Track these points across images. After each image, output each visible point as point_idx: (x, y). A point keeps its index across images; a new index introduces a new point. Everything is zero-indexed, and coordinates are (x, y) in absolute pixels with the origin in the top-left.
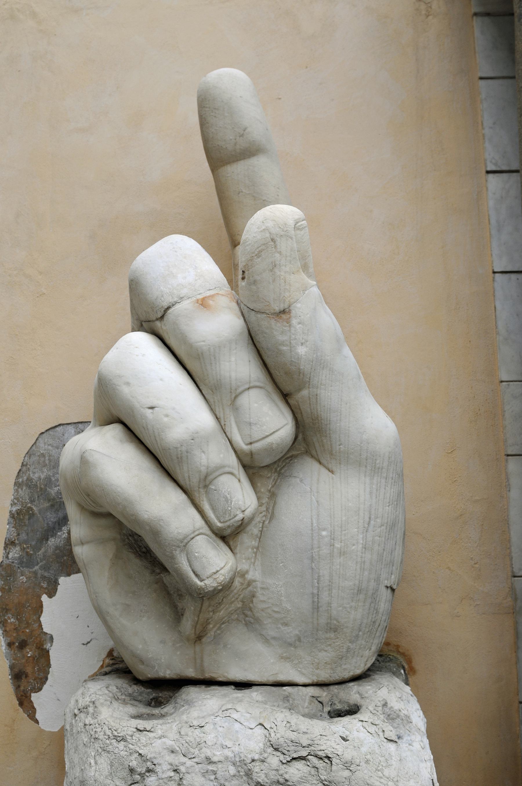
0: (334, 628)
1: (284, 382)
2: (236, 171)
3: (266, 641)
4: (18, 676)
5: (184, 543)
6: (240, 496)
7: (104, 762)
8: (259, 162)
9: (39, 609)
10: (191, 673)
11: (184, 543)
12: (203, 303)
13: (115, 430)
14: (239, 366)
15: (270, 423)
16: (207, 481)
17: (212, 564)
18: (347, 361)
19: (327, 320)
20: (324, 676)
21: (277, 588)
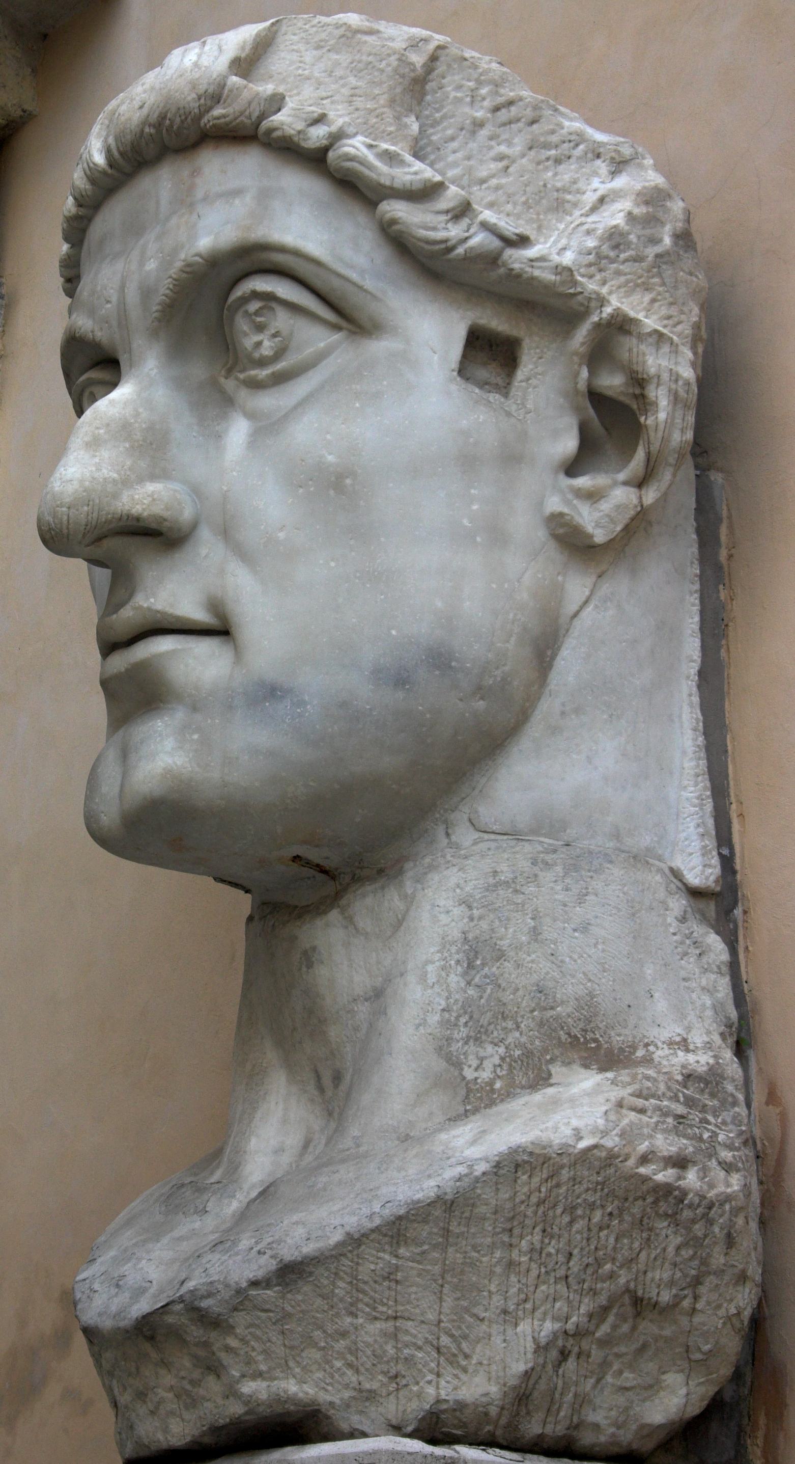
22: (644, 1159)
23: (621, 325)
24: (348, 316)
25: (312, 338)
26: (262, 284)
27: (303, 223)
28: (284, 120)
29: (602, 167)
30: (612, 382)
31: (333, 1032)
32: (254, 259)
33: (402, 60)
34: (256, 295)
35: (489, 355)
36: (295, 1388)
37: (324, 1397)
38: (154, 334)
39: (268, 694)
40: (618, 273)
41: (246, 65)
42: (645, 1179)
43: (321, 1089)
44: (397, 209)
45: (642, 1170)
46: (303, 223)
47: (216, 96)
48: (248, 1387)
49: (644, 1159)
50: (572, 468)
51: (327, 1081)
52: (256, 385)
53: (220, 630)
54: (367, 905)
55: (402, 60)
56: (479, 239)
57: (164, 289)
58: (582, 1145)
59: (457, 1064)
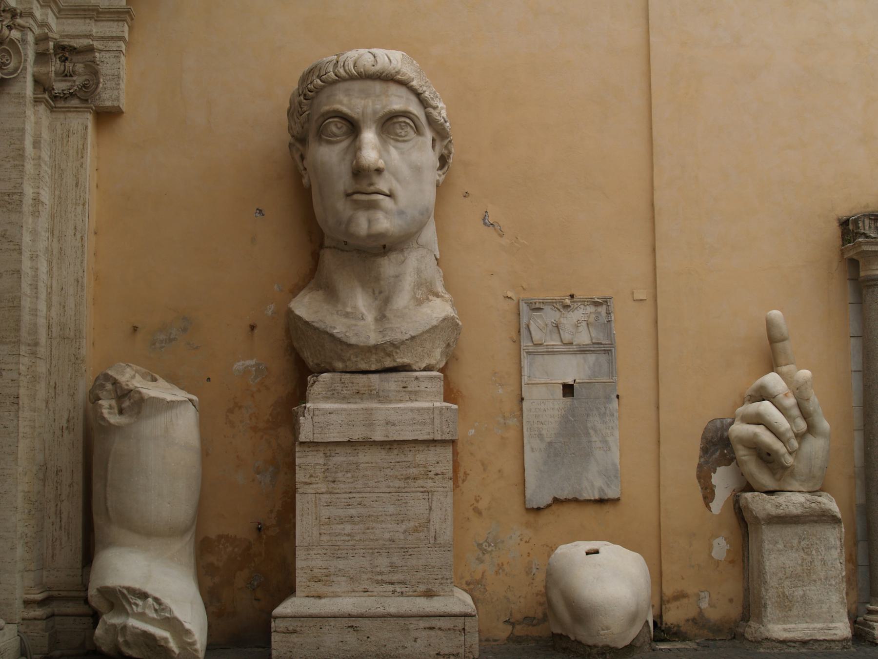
0: (814, 477)
1: (806, 415)
2: (779, 345)
3: (797, 480)
4: (705, 498)
5: (783, 455)
6: (795, 443)
7: (769, 505)
8: (786, 342)
9: (711, 477)
10: (778, 489)
11: (783, 455)
12: (786, 395)
13: (762, 427)
14: (796, 412)
15: (802, 425)
16: (789, 440)
17: (789, 460)
18: (820, 410)
19: (816, 400)
20: (810, 490)
21: (801, 467)
24: (418, 131)
25: (412, 134)
27: (415, 108)
30: (445, 152)
31: (382, 283)
32: (406, 114)
34: (405, 122)
36: (406, 360)
38: (375, 122)
39: (401, 213)
43: (374, 293)
46: (415, 108)
48: (398, 360)
51: (377, 292)
52: (397, 141)
53: (390, 195)
54: (394, 256)
57: (381, 114)
59: (415, 294)
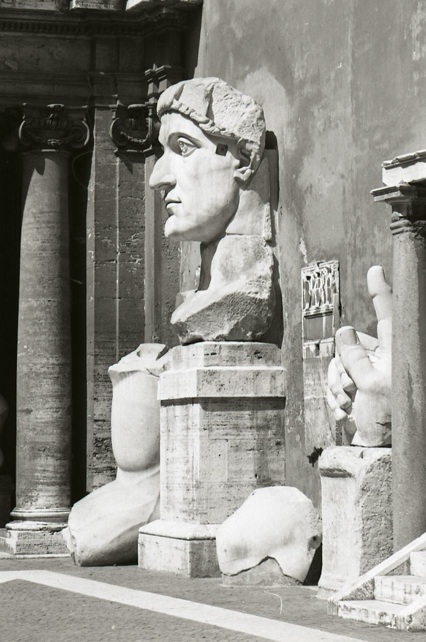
6: (344, 398)
22: (249, 293)
23: (246, 141)
26: (181, 139)
28: (182, 109)
29: (244, 106)
33: (205, 90)
35: (221, 151)
37: (202, 335)
40: (245, 129)
41: (177, 97)
42: (249, 297)
44: (201, 125)
45: (249, 295)
47: (172, 103)
49: (249, 293)
50: (240, 166)
55: (205, 90)
56: (217, 130)
58: (238, 292)
